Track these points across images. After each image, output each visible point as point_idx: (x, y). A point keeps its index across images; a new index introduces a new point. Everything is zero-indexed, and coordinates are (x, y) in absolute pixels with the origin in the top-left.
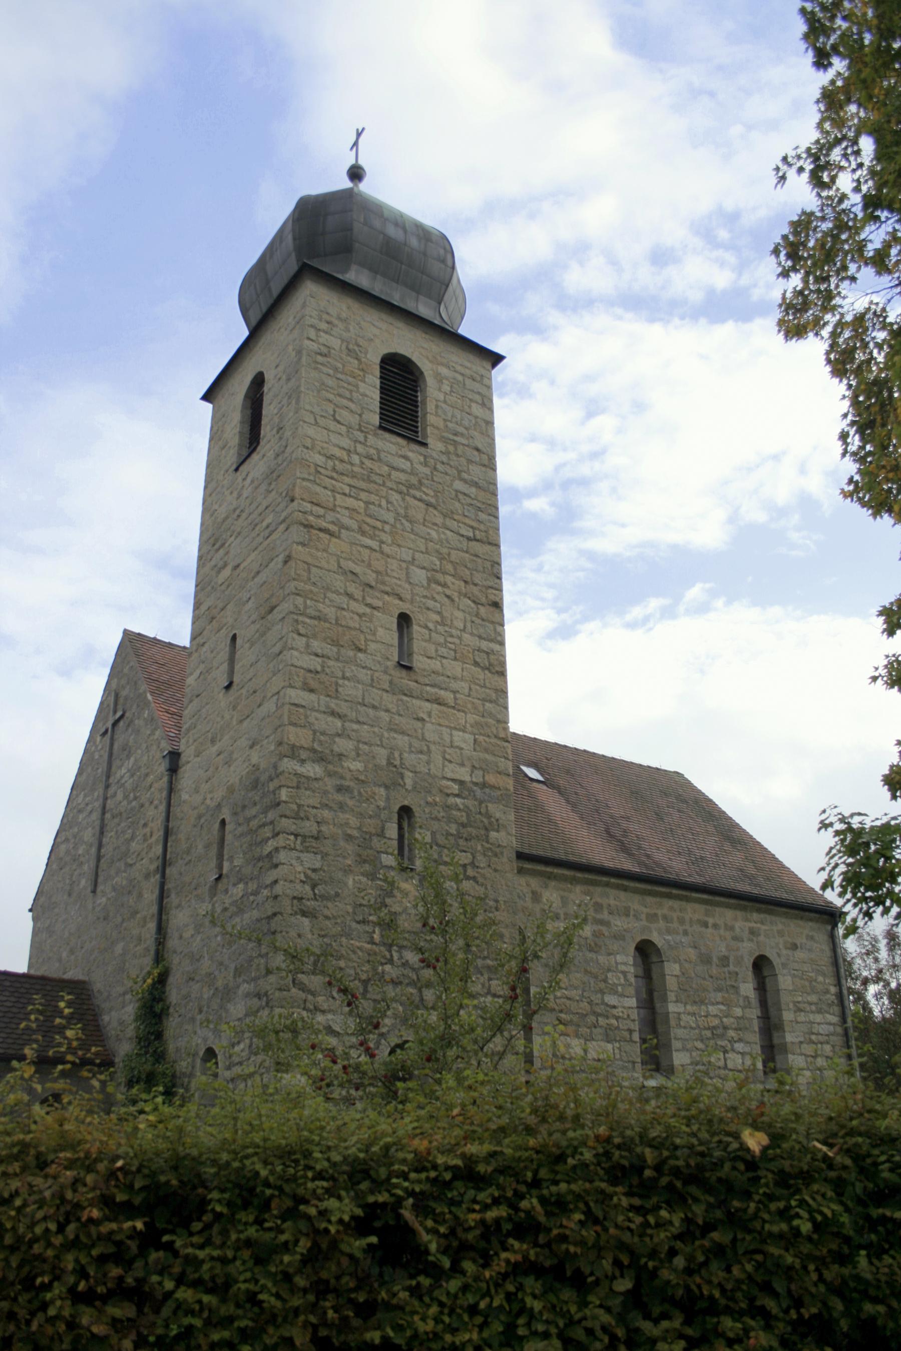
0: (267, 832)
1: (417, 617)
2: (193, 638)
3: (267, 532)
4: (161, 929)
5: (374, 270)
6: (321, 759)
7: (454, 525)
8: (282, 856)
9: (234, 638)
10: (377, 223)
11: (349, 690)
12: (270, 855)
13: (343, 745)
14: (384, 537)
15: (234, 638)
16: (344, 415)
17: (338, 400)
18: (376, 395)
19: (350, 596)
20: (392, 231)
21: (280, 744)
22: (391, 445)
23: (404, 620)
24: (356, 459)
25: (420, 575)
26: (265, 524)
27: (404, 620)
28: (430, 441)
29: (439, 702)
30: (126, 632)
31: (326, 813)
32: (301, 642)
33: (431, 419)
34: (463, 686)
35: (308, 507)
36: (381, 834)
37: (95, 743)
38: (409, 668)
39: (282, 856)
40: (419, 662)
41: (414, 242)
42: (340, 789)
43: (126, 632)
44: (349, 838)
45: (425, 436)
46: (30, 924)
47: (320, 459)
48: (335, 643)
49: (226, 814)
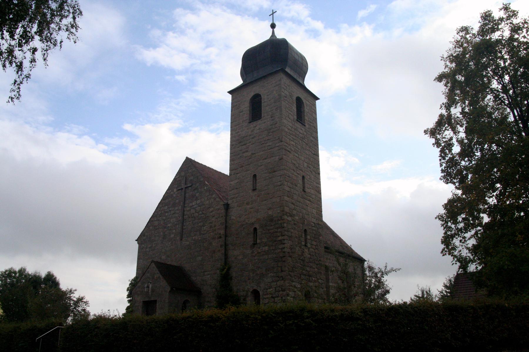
0: (279, 234)
1: (307, 177)
2: (231, 170)
3: (269, 147)
4: (226, 255)
5: (292, 69)
6: (291, 216)
7: (311, 150)
8: (286, 241)
9: (255, 176)
10: (293, 54)
11: (295, 197)
12: (281, 240)
13: (295, 212)
14: (299, 153)
15: (255, 176)
16: (290, 116)
17: (290, 112)
18: (295, 110)
19: (294, 170)
20: (297, 57)
21: (283, 211)
22: (298, 125)
23: (303, 177)
24: (293, 130)
25: (306, 164)
26: (267, 144)
27: (303, 177)
28: (306, 125)
29: (310, 201)
30: (187, 158)
31: (292, 231)
32: (286, 183)
33: (306, 118)
34: (314, 196)
35: (285, 144)
36: (302, 237)
37: (173, 191)
38: (305, 191)
39: (286, 241)
40: (307, 190)
41: (300, 60)
42: (295, 224)
43: (187, 158)
44: (296, 237)
45: (305, 123)
46: (138, 245)
47: (287, 130)
48: (292, 184)
49: (257, 226)
